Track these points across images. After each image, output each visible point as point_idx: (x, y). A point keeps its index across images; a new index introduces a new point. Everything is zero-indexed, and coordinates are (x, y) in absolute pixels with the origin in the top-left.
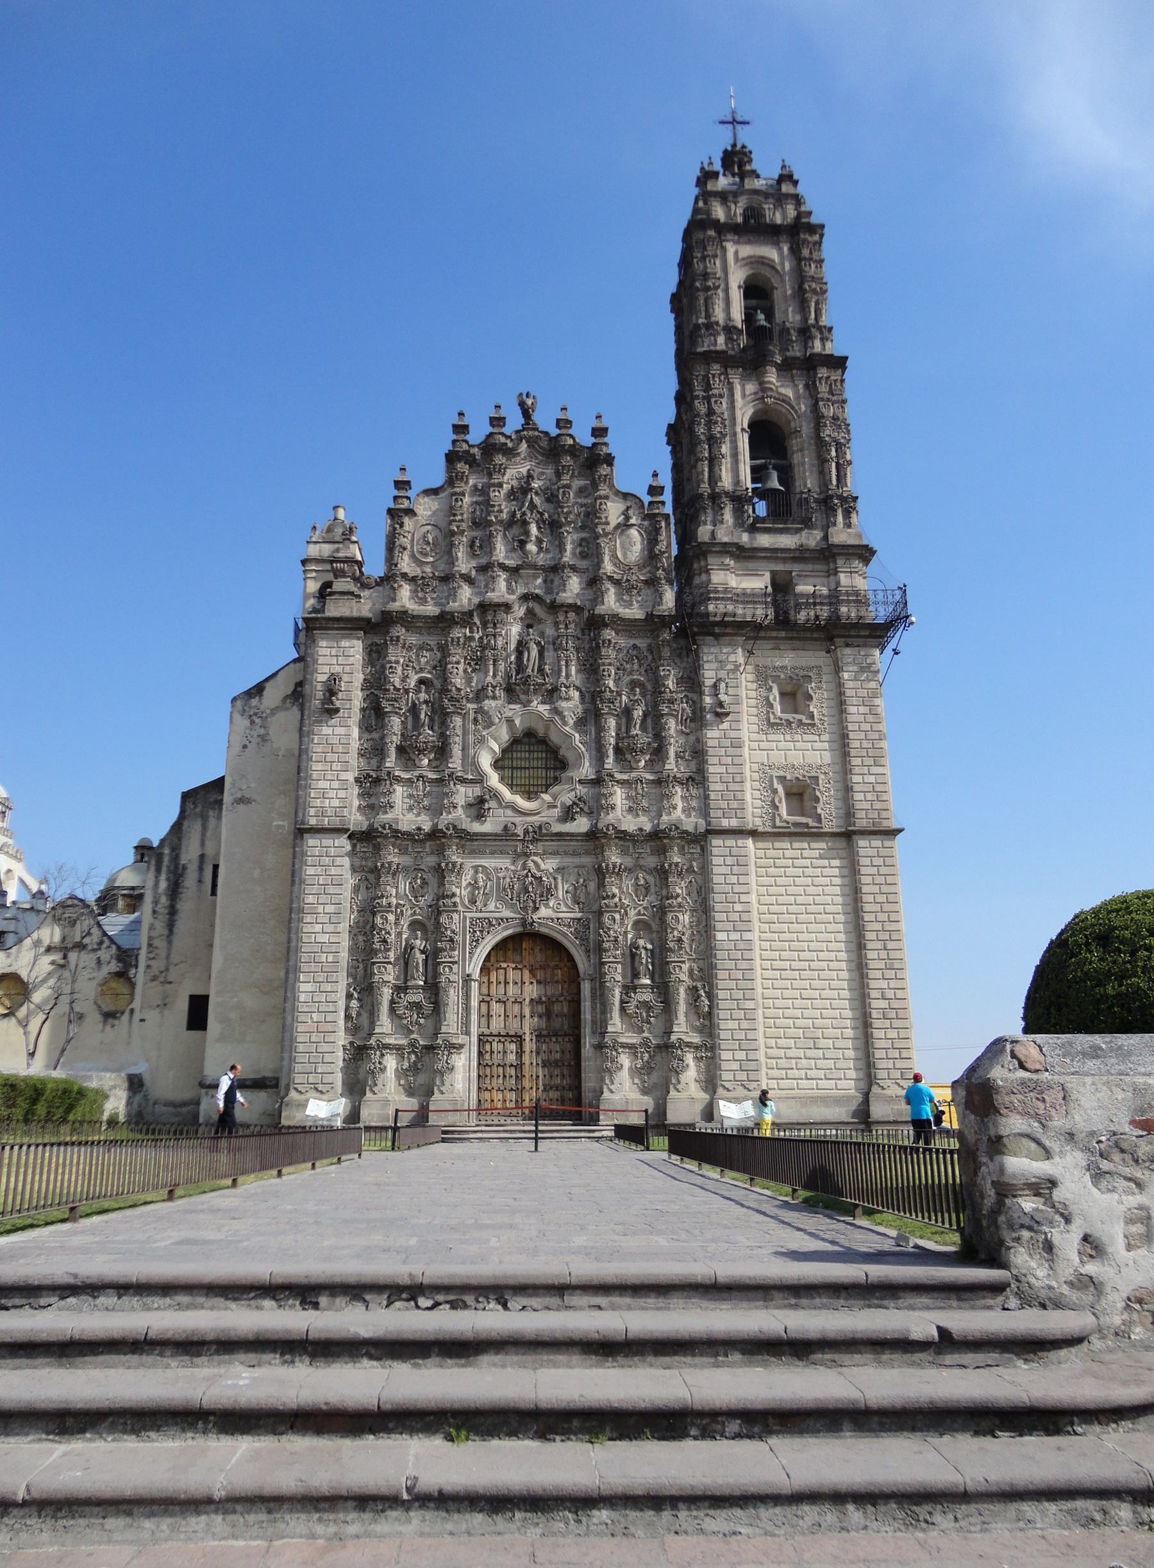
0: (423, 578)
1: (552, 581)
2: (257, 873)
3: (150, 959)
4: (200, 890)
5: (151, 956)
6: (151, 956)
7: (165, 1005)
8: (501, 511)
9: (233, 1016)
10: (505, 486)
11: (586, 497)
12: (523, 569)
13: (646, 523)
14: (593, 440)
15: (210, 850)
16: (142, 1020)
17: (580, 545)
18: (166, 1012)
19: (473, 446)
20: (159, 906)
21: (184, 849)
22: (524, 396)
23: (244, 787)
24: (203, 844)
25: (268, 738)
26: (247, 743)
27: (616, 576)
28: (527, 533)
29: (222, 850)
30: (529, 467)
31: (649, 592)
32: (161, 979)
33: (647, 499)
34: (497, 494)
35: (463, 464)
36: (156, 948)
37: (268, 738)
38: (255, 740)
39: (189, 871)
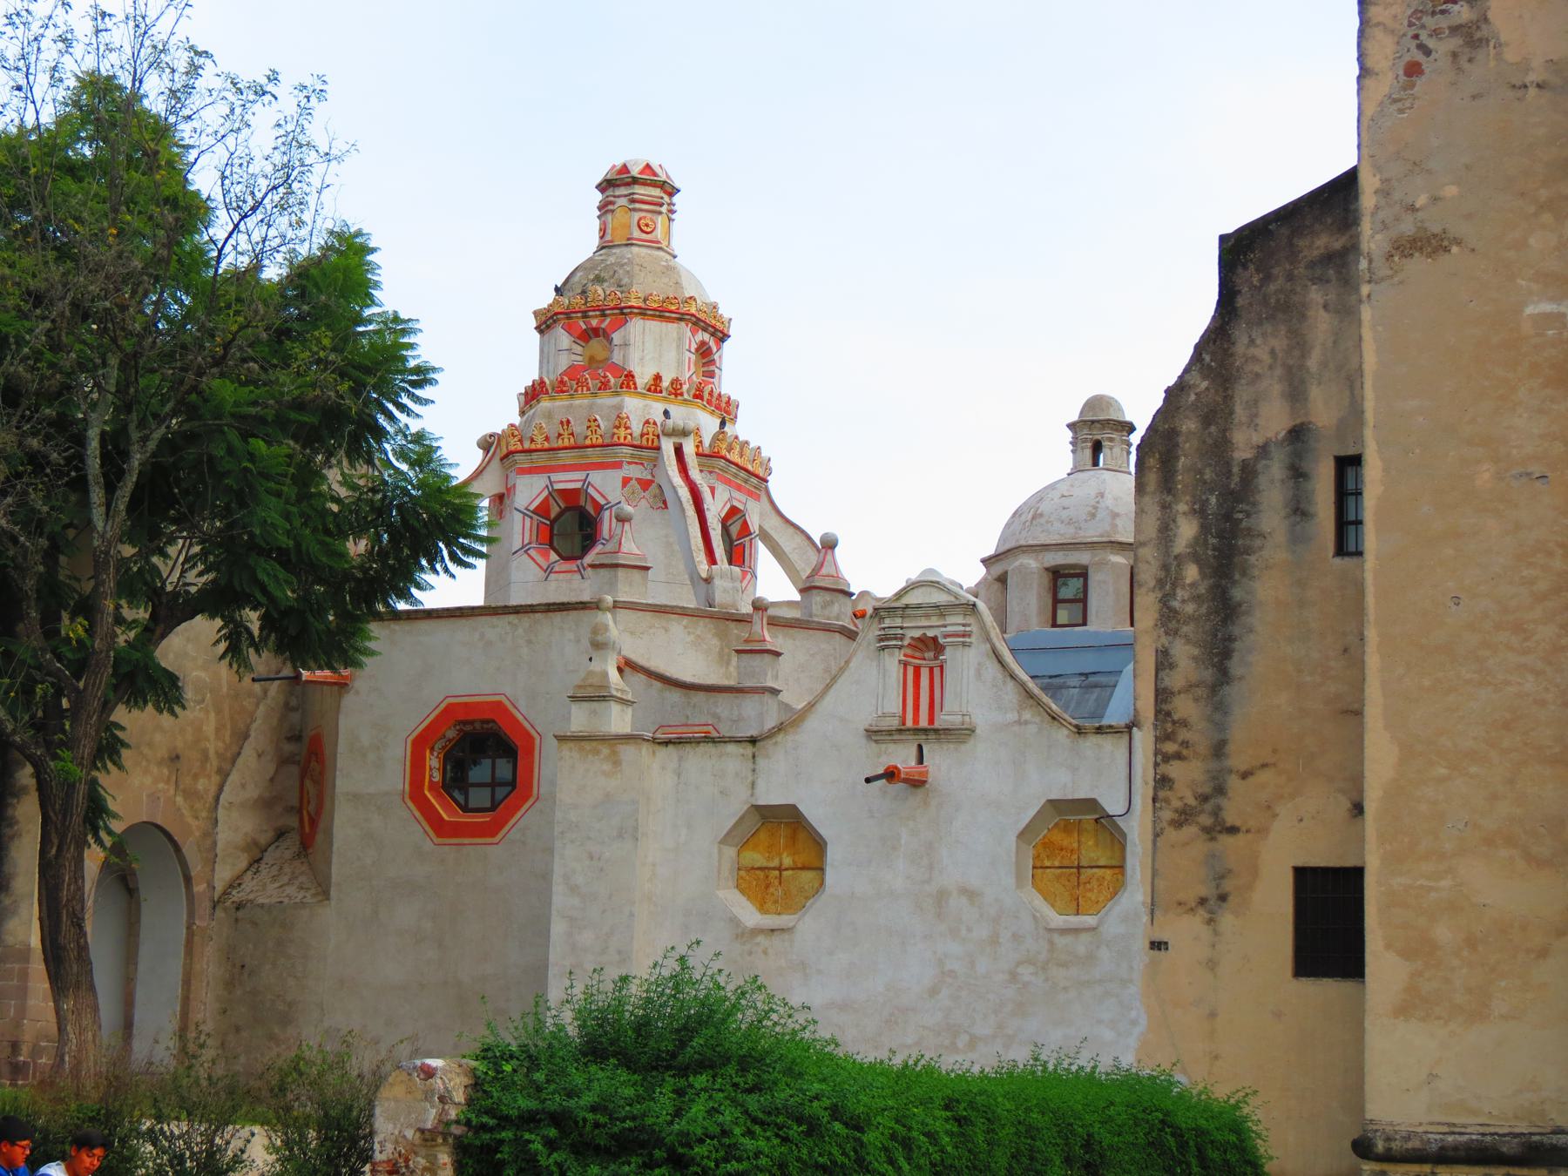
2: (1485, 475)
3: (1167, 758)
4: (1297, 539)
5: (1170, 747)
6: (1170, 747)
7: (1223, 898)
9: (1443, 933)
15: (1323, 410)
16: (1157, 945)
18: (1227, 920)
20: (1180, 593)
21: (1240, 412)
23: (1421, 201)
24: (1296, 394)
25: (1484, 32)
26: (1419, 56)
29: (1369, 405)
32: (1206, 820)
36: (1184, 723)
37: (1484, 32)
38: (1442, 48)
39: (1262, 481)
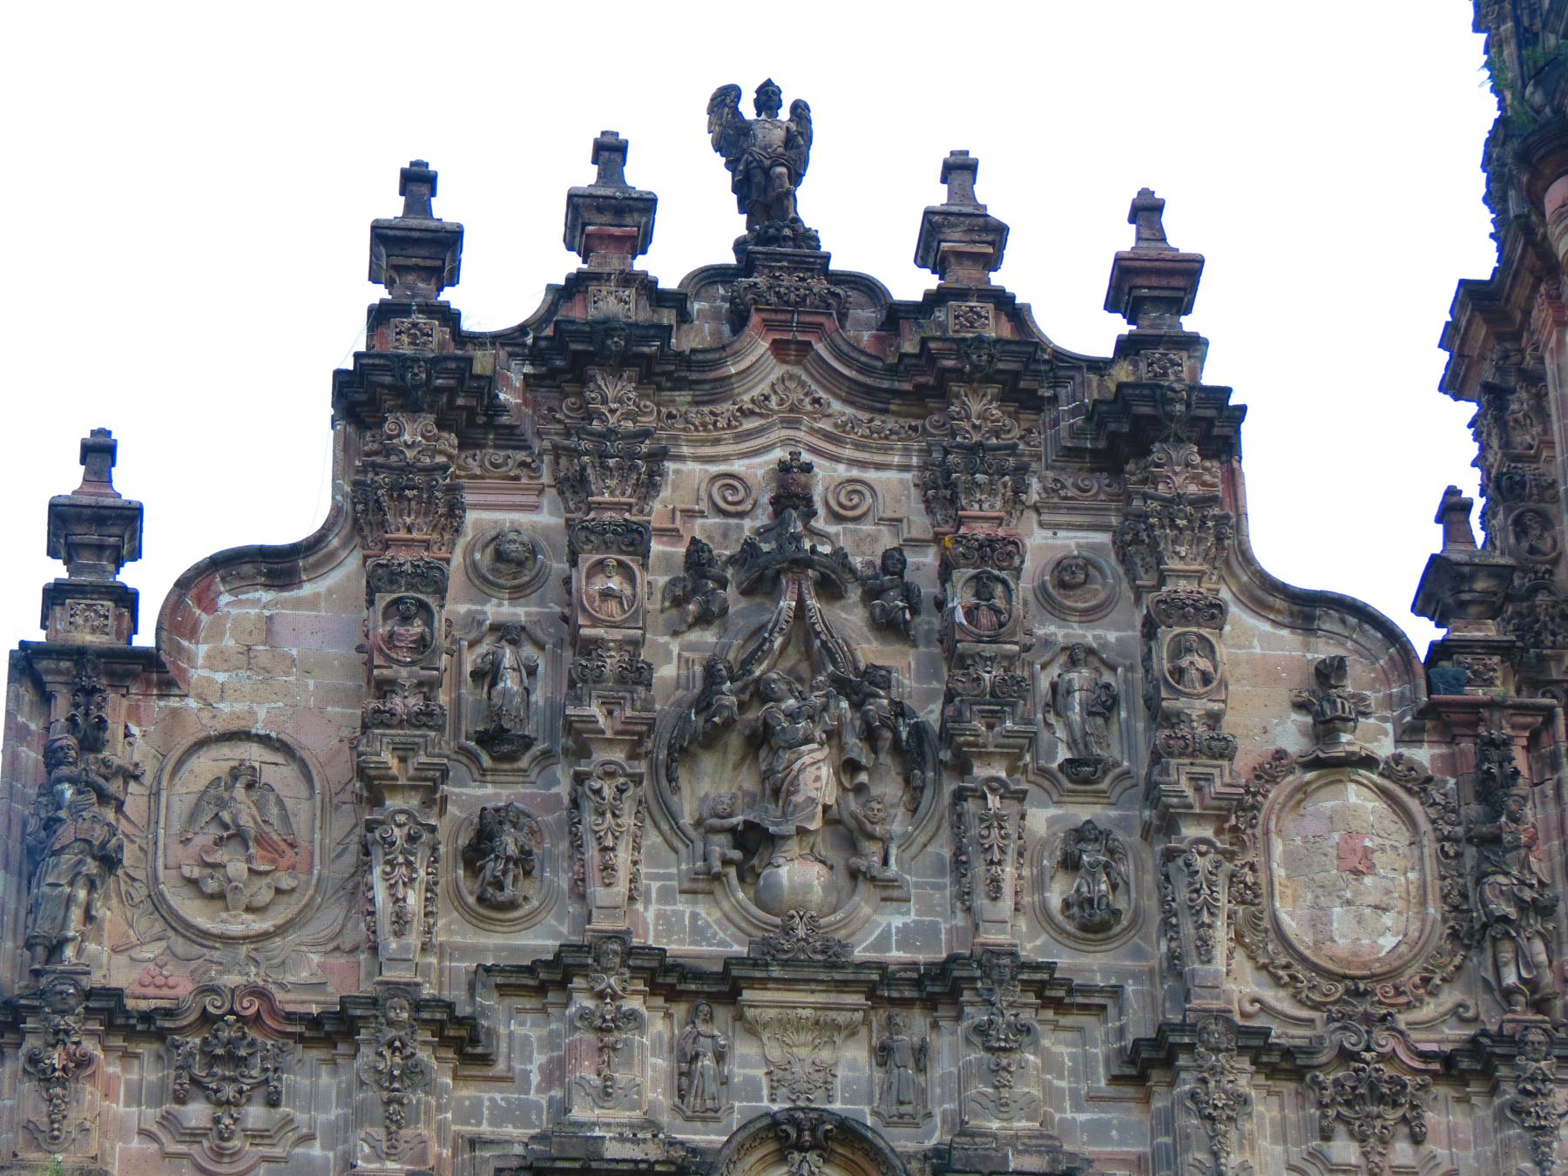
0: (206, 1019)
1: (921, 1054)
8: (637, 675)
10: (656, 547)
11: (1089, 615)
12: (763, 983)
13: (1423, 755)
14: (1119, 326)
17: (1070, 864)
19: (477, 339)
22: (747, 109)
27: (1280, 1034)
28: (778, 790)
30: (780, 454)
31: (1459, 1118)
33: (1422, 634)
34: (615, 583)
35: (428, 420)
